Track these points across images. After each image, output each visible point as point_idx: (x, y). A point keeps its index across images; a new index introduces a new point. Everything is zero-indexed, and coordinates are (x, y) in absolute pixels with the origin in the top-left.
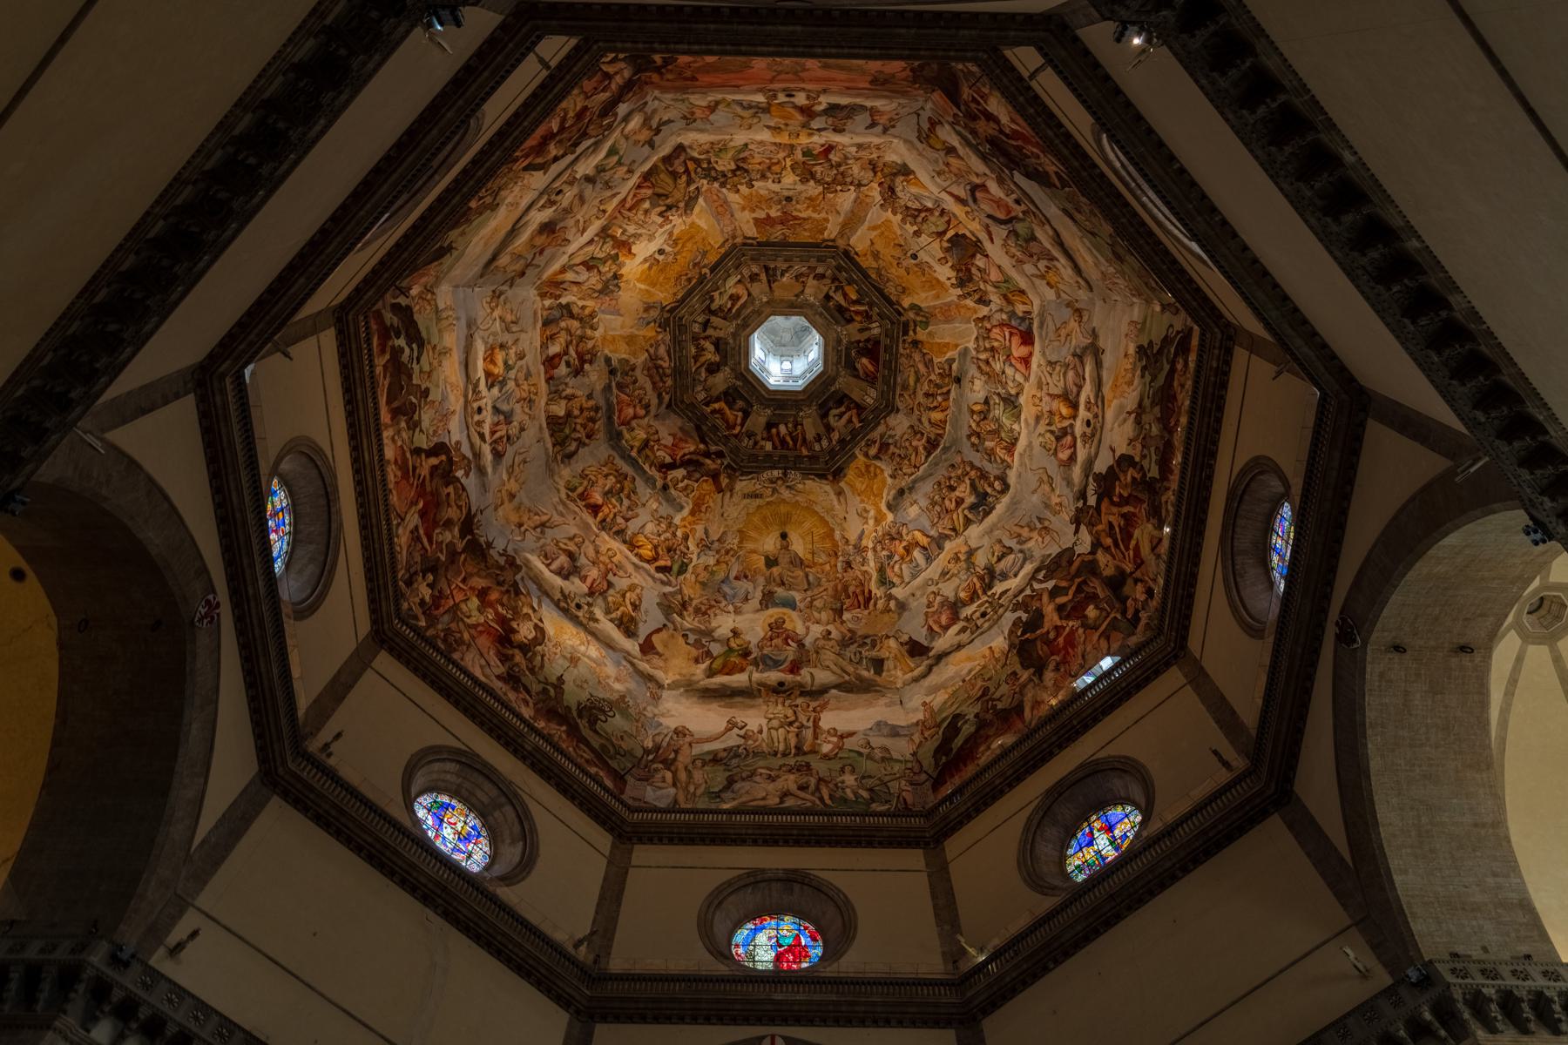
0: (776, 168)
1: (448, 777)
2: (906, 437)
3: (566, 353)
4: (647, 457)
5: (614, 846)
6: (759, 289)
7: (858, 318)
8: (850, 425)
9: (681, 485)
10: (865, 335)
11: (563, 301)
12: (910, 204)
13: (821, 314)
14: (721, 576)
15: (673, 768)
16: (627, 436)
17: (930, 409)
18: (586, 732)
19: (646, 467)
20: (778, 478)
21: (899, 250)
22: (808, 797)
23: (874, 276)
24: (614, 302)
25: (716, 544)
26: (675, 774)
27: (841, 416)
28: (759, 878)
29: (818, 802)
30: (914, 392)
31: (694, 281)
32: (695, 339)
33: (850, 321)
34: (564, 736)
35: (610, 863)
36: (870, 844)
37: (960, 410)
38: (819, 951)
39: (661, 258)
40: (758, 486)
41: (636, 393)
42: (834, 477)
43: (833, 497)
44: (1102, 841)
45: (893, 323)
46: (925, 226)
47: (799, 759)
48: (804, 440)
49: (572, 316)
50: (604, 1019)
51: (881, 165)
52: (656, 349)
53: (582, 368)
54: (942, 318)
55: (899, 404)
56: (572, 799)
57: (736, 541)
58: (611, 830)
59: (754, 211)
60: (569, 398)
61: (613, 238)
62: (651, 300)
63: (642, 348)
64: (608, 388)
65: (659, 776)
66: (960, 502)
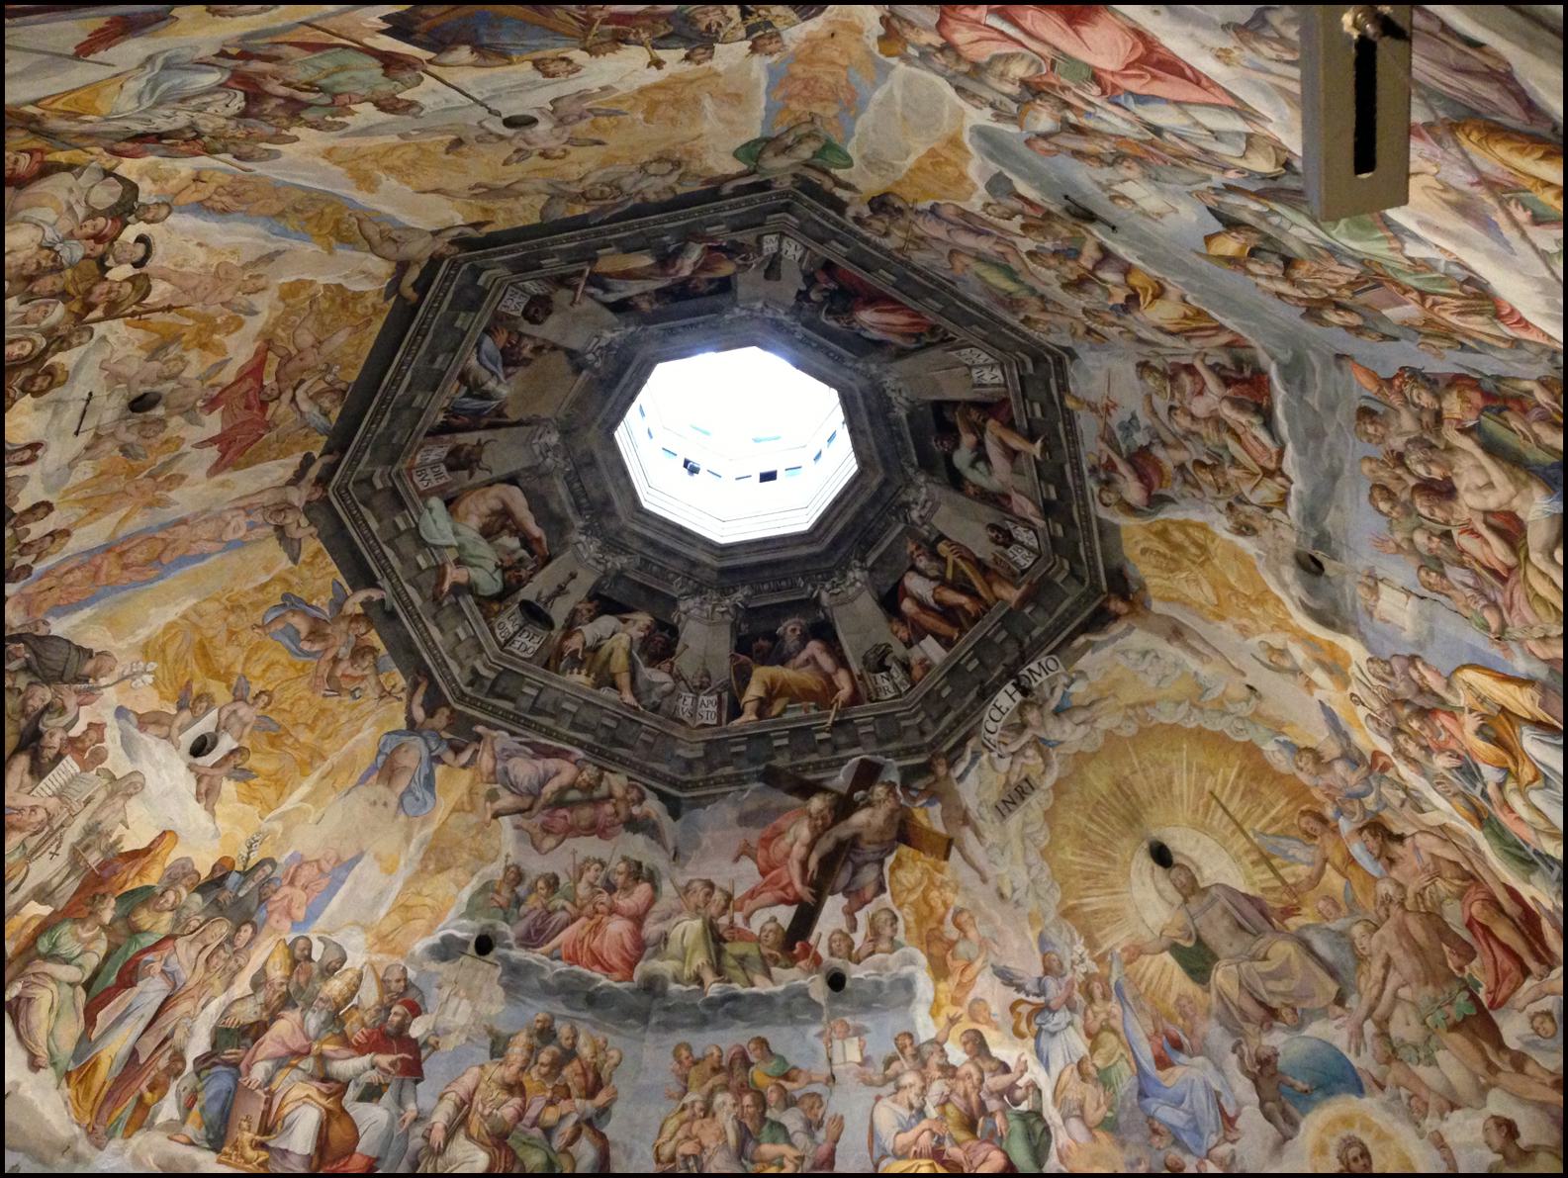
2: (1161, 403)
3: (336, 1087)
4: (742, 960)
6: (503, 453)
8: (1022, 461)
9: (859, 938)
10: (791, 282)
11: (198, 1045)
13: (672, 331)
14: (1125, 1080)
16: (664, 966)
19: (763, 987)
20: (1021, 709)
24: (307, 873)
25: (1051, 984)
27: (981, 455)
30: (1042, 297)
31: (374, 639)
32: (552, 659)
39: (227, 743)
40: (1004, 765)
41: (583, 890)
42: (1125, 598)
43: (1172, 651)
45: (787, 208)
48: (980, 565)
49: (256, 1031)
52: (511, 786)
53: (414, 1046)
57: (1080, 948)
60: (459, 1123)
61: (46, 926)
62: (366, 758)
63: (482, 828)
64: (515, 977)
66: (1510, 529)
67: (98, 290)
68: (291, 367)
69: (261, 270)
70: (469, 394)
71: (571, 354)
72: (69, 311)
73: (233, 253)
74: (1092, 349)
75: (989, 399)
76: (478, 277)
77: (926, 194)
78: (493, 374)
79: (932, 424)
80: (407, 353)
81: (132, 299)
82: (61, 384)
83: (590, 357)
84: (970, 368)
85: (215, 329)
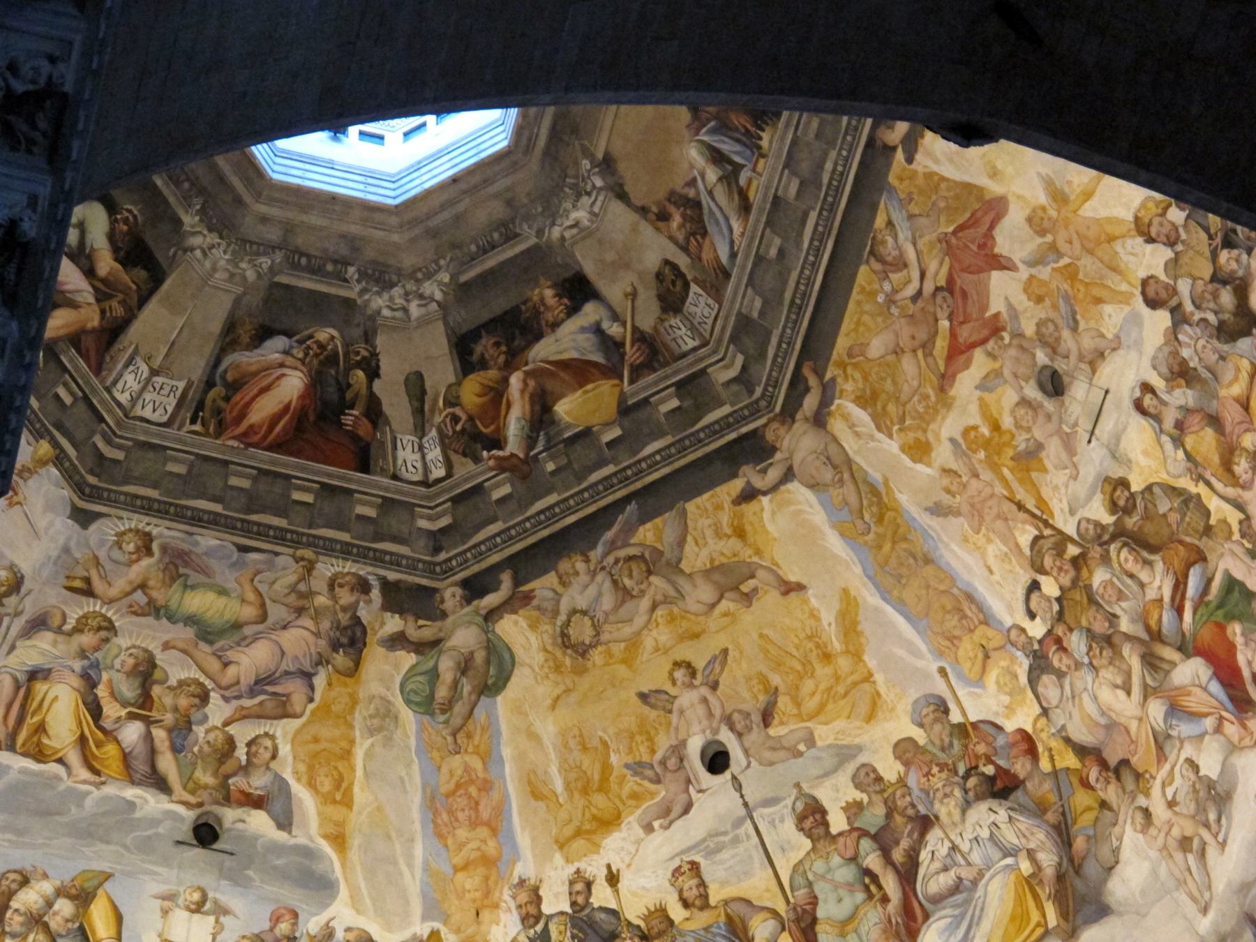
0: (1204, 441)
7: (471, 392)
10: (396, 407)
12: (935, 842)
17: (89, 681)
21: (752, 702)
23: (646, 534)
30: (155, 610)
33: (467, 361)
37: (88, 832)
45: (437, 540)
46: (846, 874)
51: (1111, 793)
54: (444, 789)
55: (105, 530)
59: (1037, 223)
67: (1066, 580)
68: (922, 335)
69: (946, 499)
70: (738, 168)
71: (622, 196)
72: (1091, 573)
73: (966, 540)
74: (66, 550)
75: (117, 346)
76: (744, 368)
77: (325, 711)
78: (710, 193)
79: (149, 239)
80: (810, 282)
81: (1046, 544)
82: (1107, 480)
83: (599, 183)
84: (154, 372)
85: (987, 444)
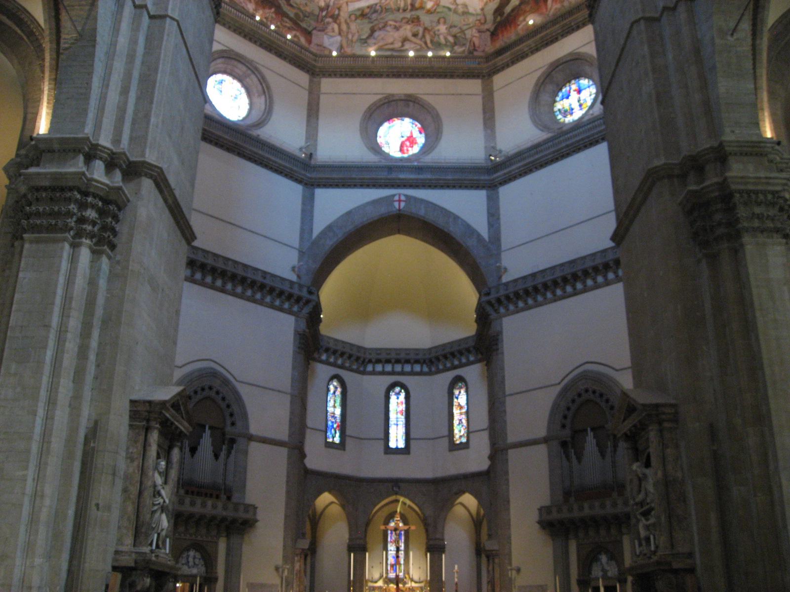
1: (220, 66)
5: (311, 81)
15: (338, 21)
18: (286, 8)
22: (418, 41)
26: (339, 25)
28: (391, 99)
29: (424, 45)
34: (274, 16)
35: (311, 92)
36: (452, 76)
38: (421, 139)
44: (574, 96)
47: (413, 13)
50: (319, 186)
56: (285, 59)
58: (308, 72)
65: (330, 27)
